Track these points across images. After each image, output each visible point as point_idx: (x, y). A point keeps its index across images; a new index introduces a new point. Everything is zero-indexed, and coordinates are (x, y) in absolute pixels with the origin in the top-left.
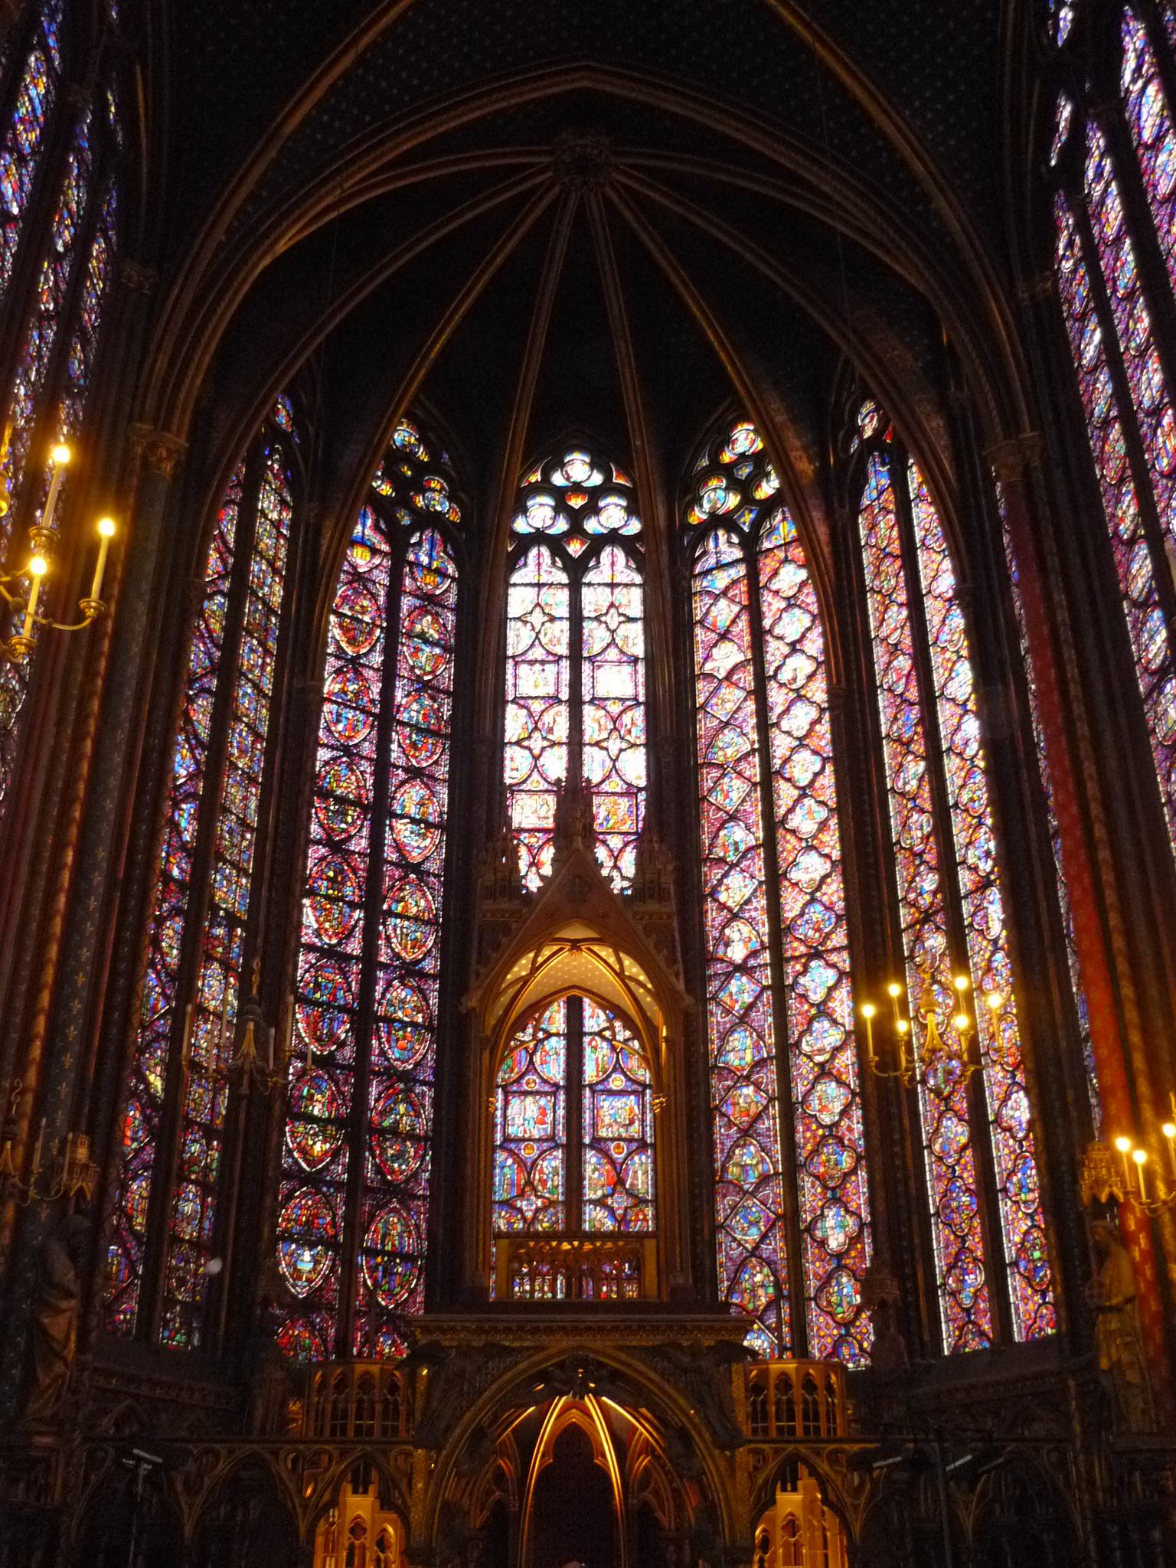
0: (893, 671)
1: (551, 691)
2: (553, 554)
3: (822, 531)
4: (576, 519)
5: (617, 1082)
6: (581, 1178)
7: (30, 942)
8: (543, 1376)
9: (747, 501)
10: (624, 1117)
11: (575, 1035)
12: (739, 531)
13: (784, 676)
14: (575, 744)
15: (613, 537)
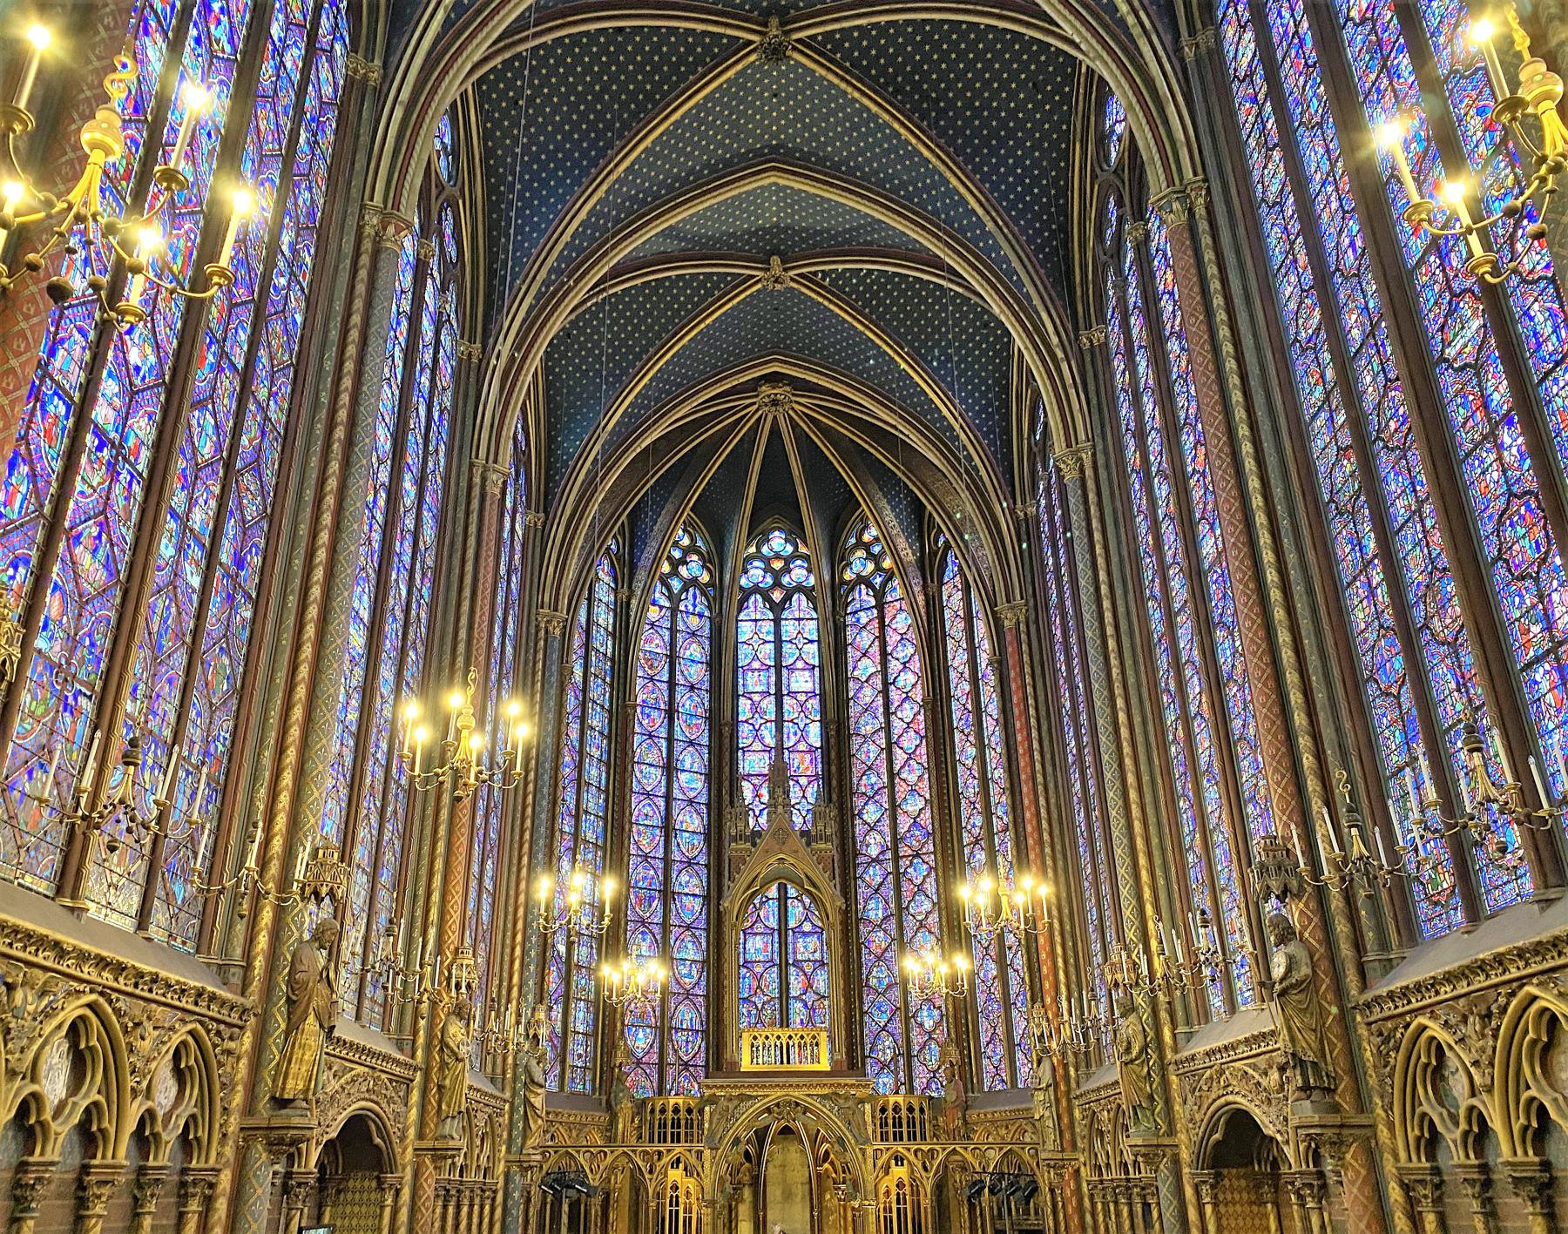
0: (960, 689)
1: (764, 688)
2: (764, 600)
3: (921, 599)
4: (777, 576)
5: (807, 927)
6: (788, 984)
7: (511, 909)
8: (769, 1110)
9: (878, 568)
10: (811, 948)
11: (783, 899)
12: (873, 588)
13: (900, 684)
14: (779, 721)
15: (799, 588)
